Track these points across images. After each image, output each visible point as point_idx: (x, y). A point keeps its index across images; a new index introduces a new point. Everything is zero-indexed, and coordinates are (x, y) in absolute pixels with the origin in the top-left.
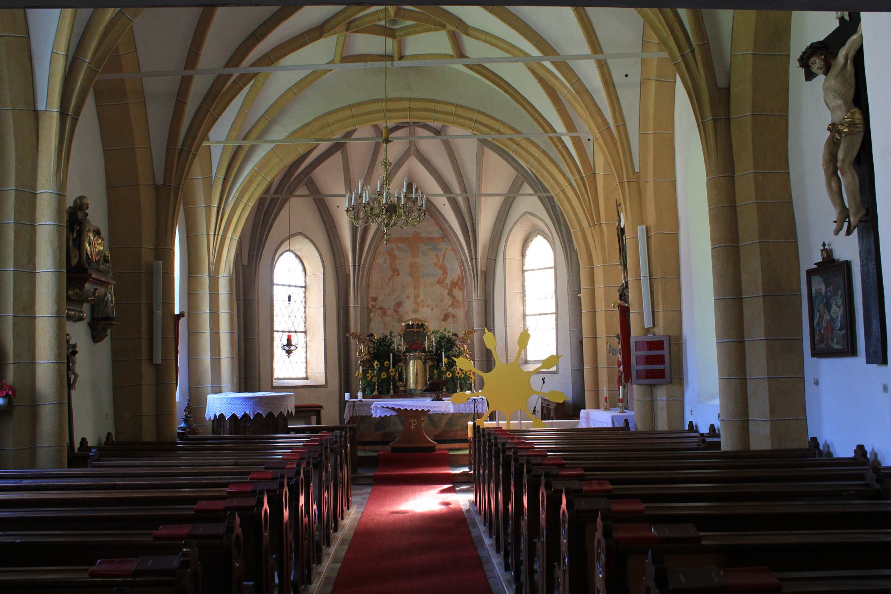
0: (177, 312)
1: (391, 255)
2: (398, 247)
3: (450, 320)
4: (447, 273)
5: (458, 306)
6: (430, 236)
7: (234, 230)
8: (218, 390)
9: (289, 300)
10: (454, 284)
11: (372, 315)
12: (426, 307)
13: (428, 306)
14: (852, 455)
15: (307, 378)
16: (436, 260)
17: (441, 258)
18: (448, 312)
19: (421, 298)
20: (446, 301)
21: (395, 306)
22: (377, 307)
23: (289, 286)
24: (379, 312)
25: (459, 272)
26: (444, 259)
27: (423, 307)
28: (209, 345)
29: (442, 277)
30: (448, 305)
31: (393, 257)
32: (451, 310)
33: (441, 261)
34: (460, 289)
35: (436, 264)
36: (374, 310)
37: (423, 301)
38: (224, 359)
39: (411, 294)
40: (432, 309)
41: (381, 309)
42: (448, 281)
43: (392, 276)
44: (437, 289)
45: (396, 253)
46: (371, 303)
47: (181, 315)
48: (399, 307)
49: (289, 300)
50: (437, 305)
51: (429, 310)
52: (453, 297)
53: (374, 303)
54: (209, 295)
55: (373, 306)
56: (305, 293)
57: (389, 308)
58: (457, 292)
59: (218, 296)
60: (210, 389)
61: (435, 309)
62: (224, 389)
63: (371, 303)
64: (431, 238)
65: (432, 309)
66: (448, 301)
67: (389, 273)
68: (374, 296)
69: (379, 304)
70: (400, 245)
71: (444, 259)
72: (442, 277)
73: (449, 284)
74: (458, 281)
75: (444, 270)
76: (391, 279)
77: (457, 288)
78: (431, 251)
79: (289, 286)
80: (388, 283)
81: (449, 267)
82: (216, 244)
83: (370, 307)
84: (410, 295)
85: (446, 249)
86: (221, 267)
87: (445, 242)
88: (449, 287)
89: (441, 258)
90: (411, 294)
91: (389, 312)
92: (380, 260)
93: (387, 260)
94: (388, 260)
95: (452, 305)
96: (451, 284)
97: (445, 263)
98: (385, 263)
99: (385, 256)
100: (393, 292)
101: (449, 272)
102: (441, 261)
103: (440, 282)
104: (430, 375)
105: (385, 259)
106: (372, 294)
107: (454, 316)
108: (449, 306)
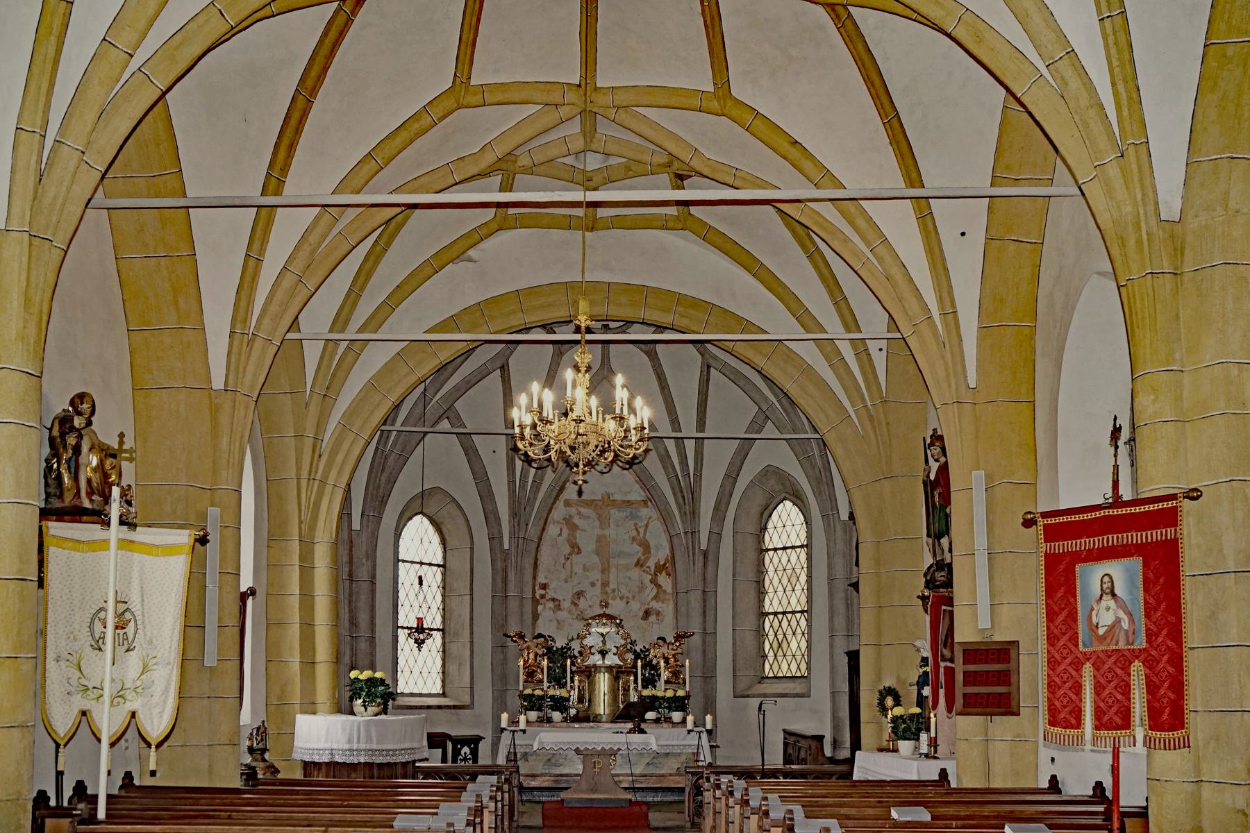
0: (244, 587)
1: (568, 521)
2: (579, 513)
3: (653, 618)
4: (650, 552)
5: (665, 599)
6: (628, 498)
7: (339, 473)
8: (310, 708)
9: (421, 583)
10: (660, 568)
11: (540, 608)
12: (618, 599)
13: (622, 598)
14: (1091, 793)
15: (444, 695)
16: (634, 533)
17: (642, 531)
18: (650, 606)
19: (612, 586)
20: (648, 591)
21: (573, 596)
22: (548, 597)
23: (422, 563)
24: (551, 604)
25: (667, 551)
26: (645, 531)
27: (614, 599)
28: (298, 642)
29: (643, 558)
30: (650, 598)
31: (573, 527)
32: (655, 605)
33: (641, 535)
34: (669, 575)
35: (634, 539)
36: (542, 601)
37: (614, 591)
38: (322, 664)
39: (598, 580)
40: (627, 603)
41: (553, 600)
42: (651, 563)
43: (570, 554)
44: (635, 573)
45: (576, 520)
46: (539, 592)
47: (252, 592)
48: (579, 598)
49: (421, 583)
50: (634, 597)
51: (623, 603)
52: (658, 586)
53: (543, 592)
54: (300, 569)
55: (543, 597)
56: (444, 574)
57: (564, 600)
58: (663, 580)
59: (313, 572)
60: (298, 707)
61: (632, 603)
62: (319, 707)
63: (539, 592)
64: (628, 501)
65: (627, 603)
66: (651, 591)
67: (567, 550)
68: (544, 581)
69: (550, 593)
70: (582, 510)
71: (645, 531)
72: (643, 558)
73: (653, 568)
74: (665, 564)
75: (646, 547)
76: (568, 559)
77: (664, 573)
78: (627, 520)
79: (422, 563)
80: (564, 564)
81: (652, 543)
82: (311, 492)
83: (538, 597)
84: (596, 582)
85: (650, 518)
86: (317, 528)
87: (648, 507)
88: (652, 572)
89: (642, 531)
90: (598, 580)
91: (566, 604)
92: (552, 530)
93: (564, 530)
94: (566, 532)
95: (656, 598)
96: (656, 567)
97: (647, 537)
98: (560, 535)
99: (560, 526)
100: (571, 577)
101: (653, 551)
102: (641, 535)
103: (639, 564)
104: (623, 695)
105: (561, 530)
106: (541, 579)
107: (658, 613)
108: (653, 599)
